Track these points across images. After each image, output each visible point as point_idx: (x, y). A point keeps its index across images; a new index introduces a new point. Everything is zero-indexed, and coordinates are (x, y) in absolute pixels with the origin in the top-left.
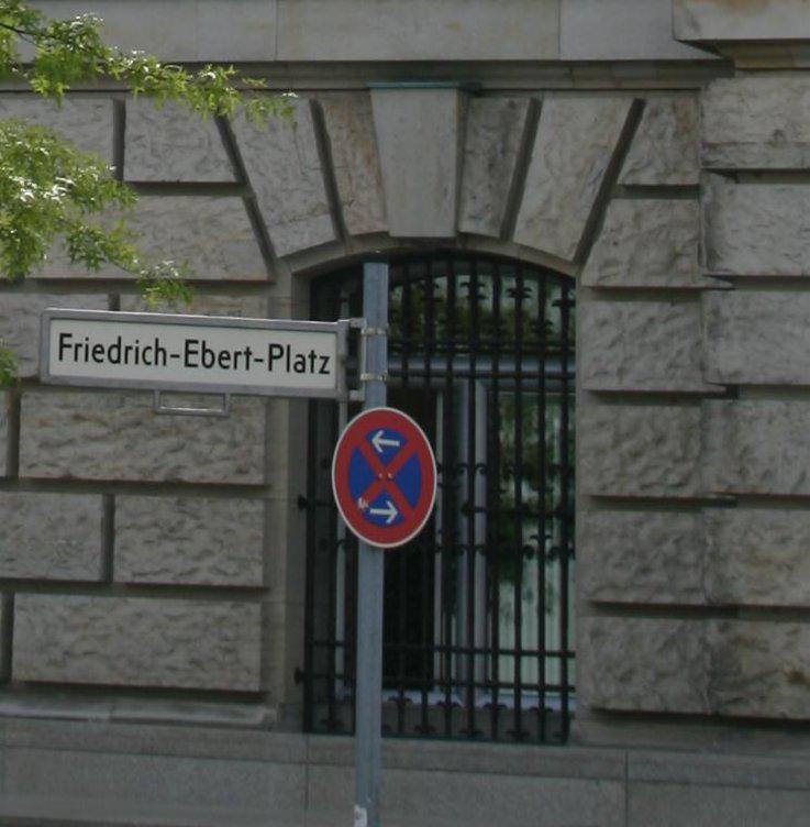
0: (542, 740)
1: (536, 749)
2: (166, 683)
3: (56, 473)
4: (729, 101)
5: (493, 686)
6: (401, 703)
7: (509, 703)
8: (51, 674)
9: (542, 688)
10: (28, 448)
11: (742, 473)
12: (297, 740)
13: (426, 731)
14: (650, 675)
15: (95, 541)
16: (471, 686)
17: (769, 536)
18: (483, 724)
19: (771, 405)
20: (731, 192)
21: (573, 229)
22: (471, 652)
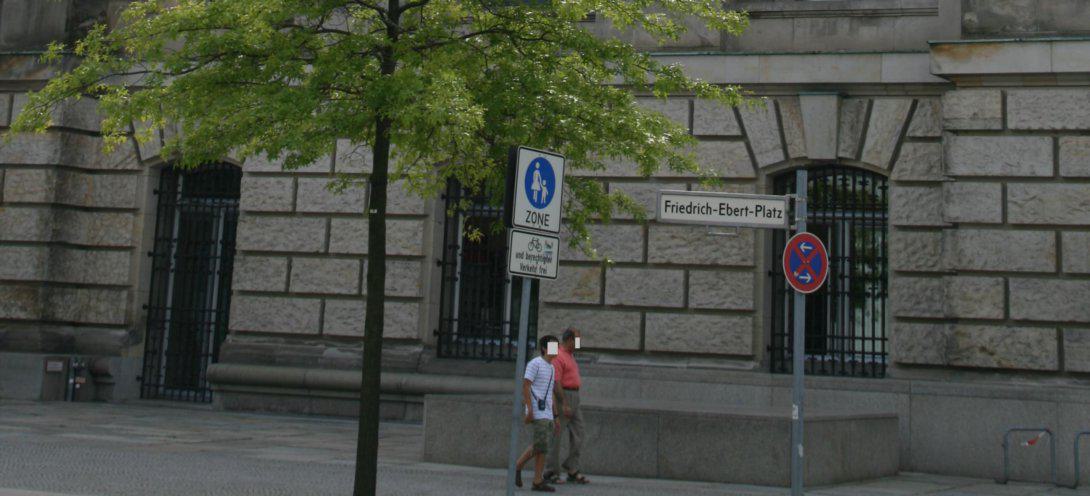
0: (874, 376)
1: (872, 380)
2: (711, 351)
3: (664, 261)
4: (954, 100)
5: (852, 352)
6: (813, 360)
7: (860, 360)
8: (661, 348)
9: (874, 354)
10: (652, 250)
11: (960, 261)
12: (768, 376)
13: (823, 372)
14: (920, 348)
15: (681, 290)
16: (843, 353)
17: (971, 288)
18: (848, 369)
19: (972, 232)
20: (955, 140)
21: (886, 156)
22: (843, 338)
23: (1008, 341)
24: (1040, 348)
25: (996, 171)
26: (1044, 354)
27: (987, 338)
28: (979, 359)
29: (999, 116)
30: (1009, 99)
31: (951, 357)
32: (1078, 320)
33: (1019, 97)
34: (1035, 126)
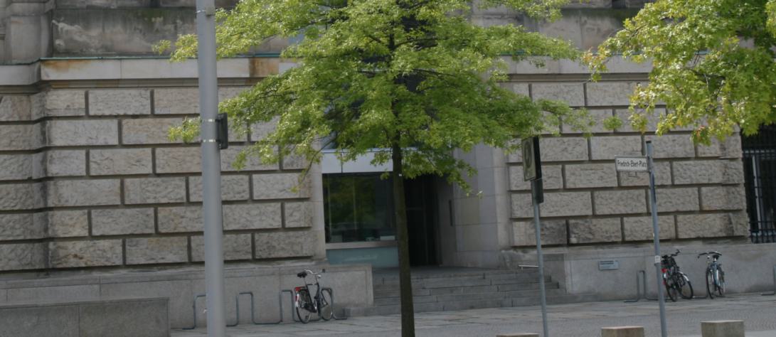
4: (54, 97)
11: (59, 201)
14: (6, 260)
17: (68, 218)
19: (67, 182)
20: (55, 123)
23: (92, 249)
24: (110, 251)
25: (83, 142)
26: (114, 255)
27: (77, 248)
28: (73, 263)
29: (84, 107)
30: (91, 96)
31: (55, 262)
32: (136, 233)
33: (95, 94)
34: (107, 113)
